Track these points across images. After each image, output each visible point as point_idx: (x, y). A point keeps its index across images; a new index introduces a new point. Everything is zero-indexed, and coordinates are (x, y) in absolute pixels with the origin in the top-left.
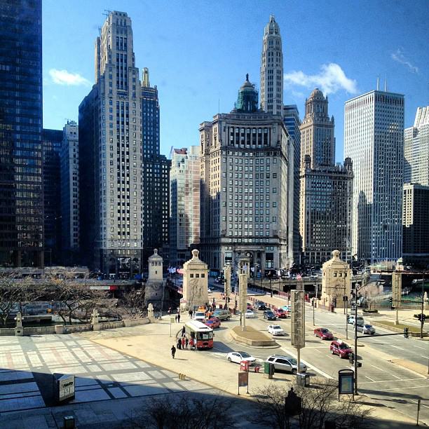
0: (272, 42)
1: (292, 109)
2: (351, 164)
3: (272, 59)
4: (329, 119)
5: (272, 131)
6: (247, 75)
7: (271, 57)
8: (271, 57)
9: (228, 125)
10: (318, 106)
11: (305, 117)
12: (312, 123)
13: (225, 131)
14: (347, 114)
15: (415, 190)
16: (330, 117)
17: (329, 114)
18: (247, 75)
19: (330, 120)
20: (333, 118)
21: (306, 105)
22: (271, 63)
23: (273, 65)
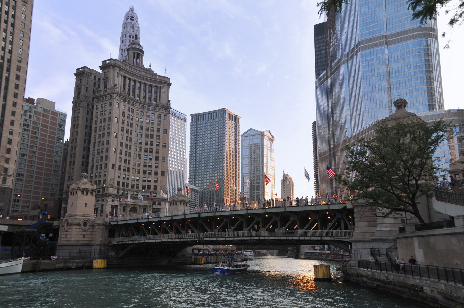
0: (133, 27)
5: (162, 90)
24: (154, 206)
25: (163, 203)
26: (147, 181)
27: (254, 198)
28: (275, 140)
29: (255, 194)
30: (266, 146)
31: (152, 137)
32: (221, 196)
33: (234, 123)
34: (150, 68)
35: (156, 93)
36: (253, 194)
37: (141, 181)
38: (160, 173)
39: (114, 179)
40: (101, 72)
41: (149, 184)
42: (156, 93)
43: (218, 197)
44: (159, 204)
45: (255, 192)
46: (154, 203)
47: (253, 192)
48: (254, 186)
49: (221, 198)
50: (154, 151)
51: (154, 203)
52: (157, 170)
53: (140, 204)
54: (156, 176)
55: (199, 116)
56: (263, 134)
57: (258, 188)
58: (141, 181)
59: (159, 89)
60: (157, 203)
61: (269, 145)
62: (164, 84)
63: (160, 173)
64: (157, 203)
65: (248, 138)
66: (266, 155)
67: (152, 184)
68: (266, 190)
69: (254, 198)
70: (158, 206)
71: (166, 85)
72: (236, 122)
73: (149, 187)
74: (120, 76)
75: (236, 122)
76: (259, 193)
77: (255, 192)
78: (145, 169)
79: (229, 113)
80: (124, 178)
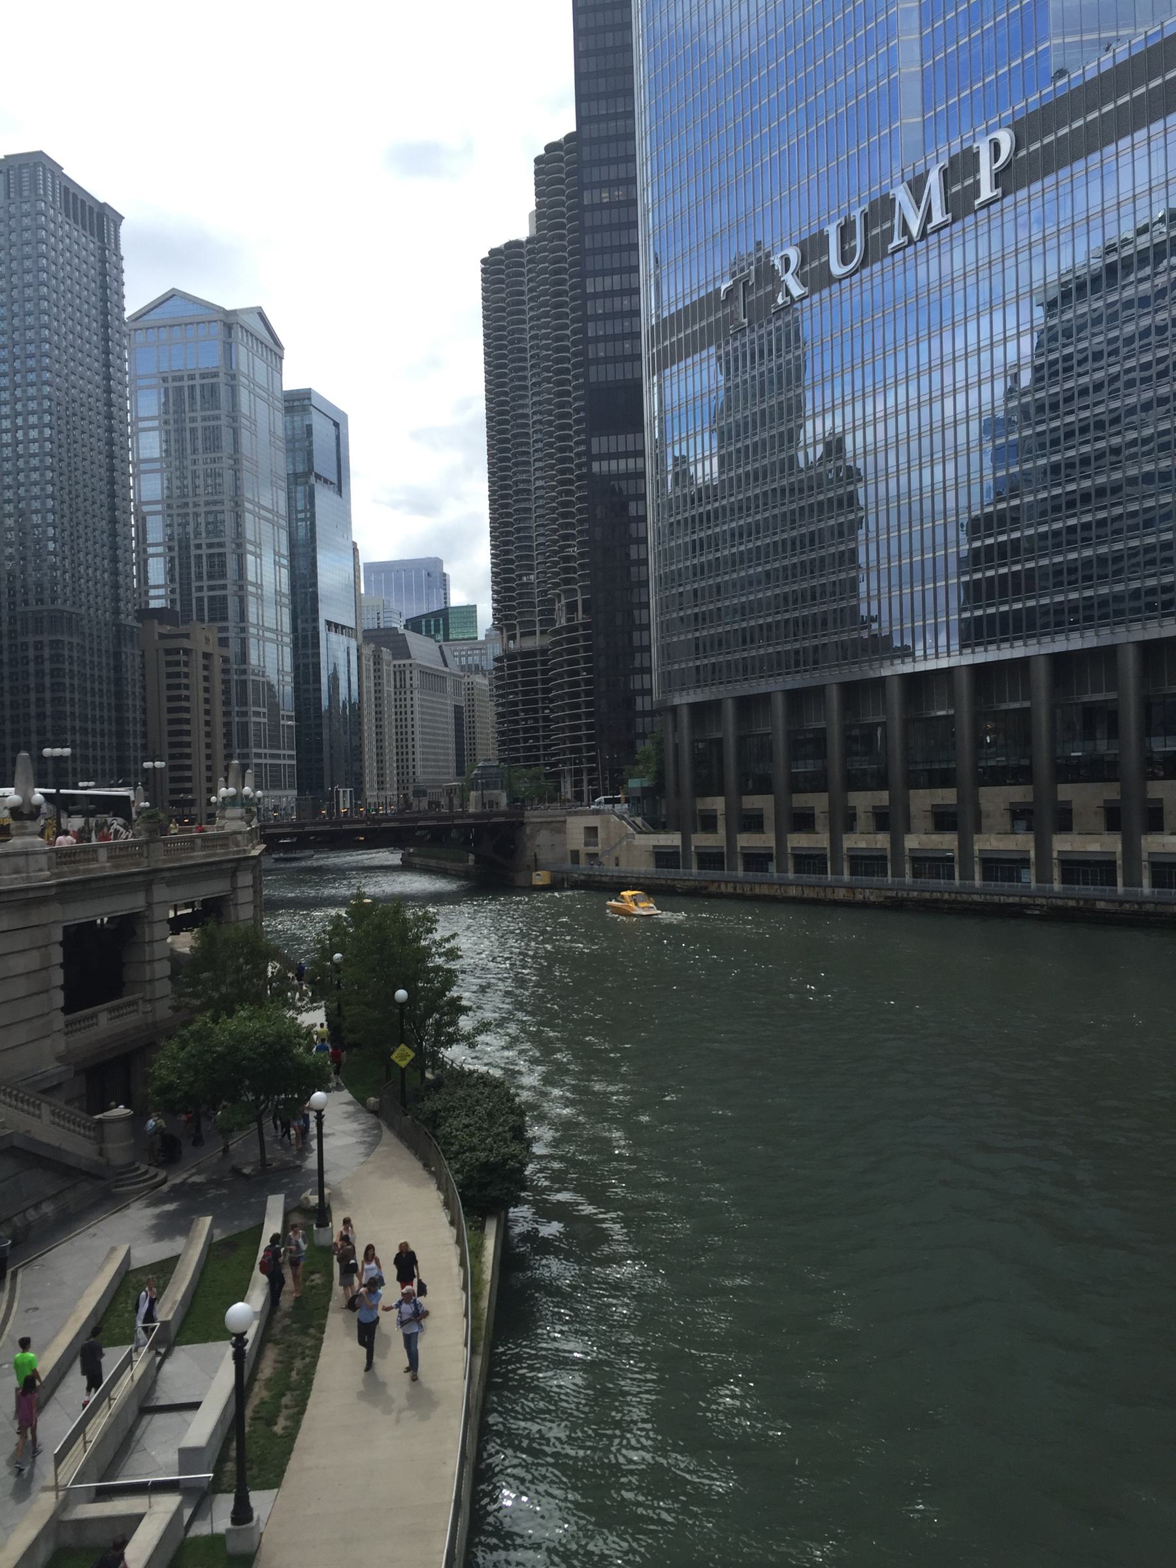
27: (200, 609)
28: (287, 354)
29: (206, 594)
30: (247, 377)
32: (40, 601)
36: (195, 595)
43: (26, 603)
45: (205, 583)
47: (194, 584)
48: (199, 557)
49: (40, 607)
56: (231, 320)
57: (217, 565)
61: (261, 376)
65: (164, 333)
66: (249, 418)
68: (251, 576)
69: (200, 609)
76: (224, 587)
77: (205, 583)
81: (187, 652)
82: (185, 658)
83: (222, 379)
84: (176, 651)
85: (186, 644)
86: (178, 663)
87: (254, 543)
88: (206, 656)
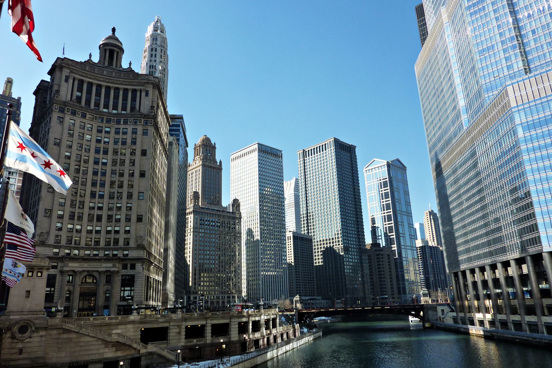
0: (156, 39)
1: (179, 118)
2: (239, 206)
3: (156, 55)
4: (217, 163)
5: (143, 94)
6: (114, 30)
7: (154, 53)
8: (154, 53)
9: (73, 75)
10: (206, 150)
11: (194, 160)
12: (201, 163)
13: (67, 80)
14: (232, 164)
15: (294, 237)
16: (218, 162)
17: (216, 158)
18: (114, 30)
19: (218, 164)
20: (221, 162)
21: (195, 149)
22: (153, 58)
23: (155, 61)
24: (124, 272)
25: (139, 266)
26: (113, 232)
31: (123, 163)
33: (348, 154)
34: (130, 68)
35: (134, 99)
37: (103, 233)
38: (134, 218)
39: (48, 233)
40: (49, 80)
41: (117, 236)
42: (134, 99)
43: (336, 245)
44: (133, 267)
46: (125, 267)
50: (125, 185)
51: (125, 267)
52: (129, 213)
53: (100, 270)
54: (128, 224)
55: (306, 152)
58: (103, 233)
59: (138, 94)
60: (129, 266)
62: (146, 85)
63: (134, 218)
64: (129, 266)
67: (122, 237)
70: (131, 271)
71: (152, 86)
72: (351, 153)
73: (116, 241)
74: (71, 81)
75: (351, 153)
78: (110, 213)
79: (340, 143)
80: (71, 230)
81: (382, 255)
82: (381, 256)
83: (388, 180)
84: (379, 255)
85: (381, 252)
86: (379, 258)
87: (401, 222)
88: (388, 255)
